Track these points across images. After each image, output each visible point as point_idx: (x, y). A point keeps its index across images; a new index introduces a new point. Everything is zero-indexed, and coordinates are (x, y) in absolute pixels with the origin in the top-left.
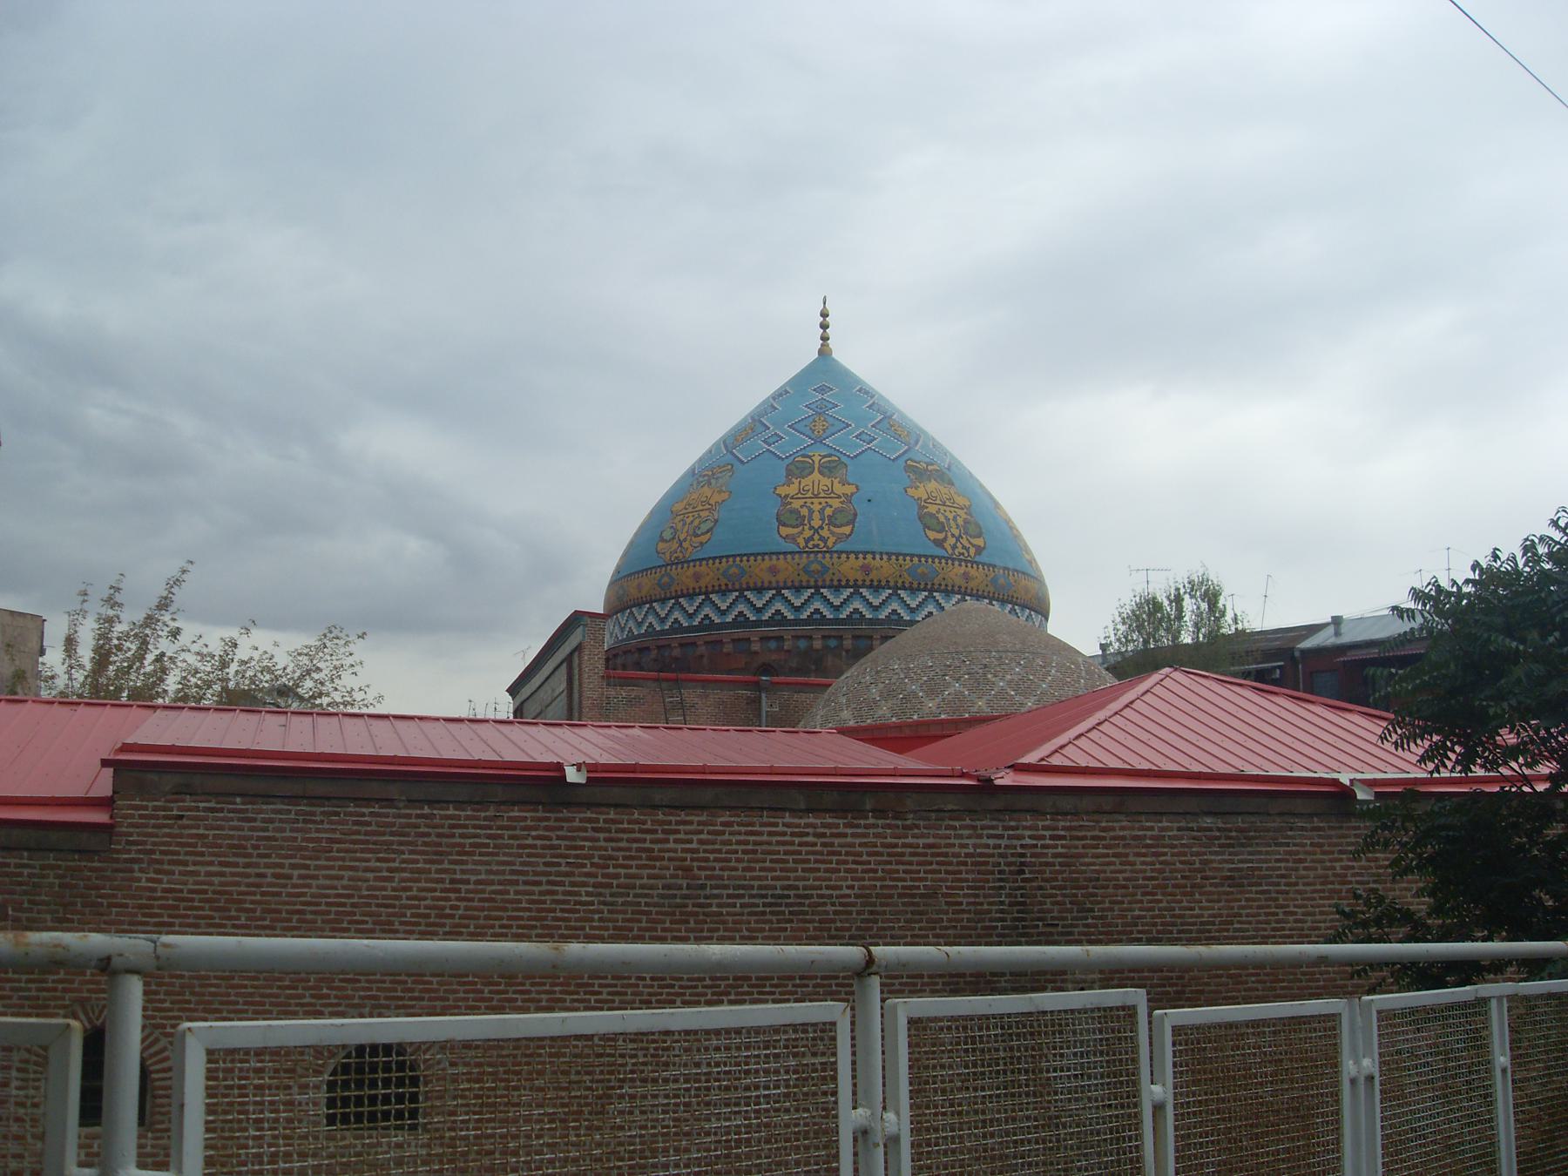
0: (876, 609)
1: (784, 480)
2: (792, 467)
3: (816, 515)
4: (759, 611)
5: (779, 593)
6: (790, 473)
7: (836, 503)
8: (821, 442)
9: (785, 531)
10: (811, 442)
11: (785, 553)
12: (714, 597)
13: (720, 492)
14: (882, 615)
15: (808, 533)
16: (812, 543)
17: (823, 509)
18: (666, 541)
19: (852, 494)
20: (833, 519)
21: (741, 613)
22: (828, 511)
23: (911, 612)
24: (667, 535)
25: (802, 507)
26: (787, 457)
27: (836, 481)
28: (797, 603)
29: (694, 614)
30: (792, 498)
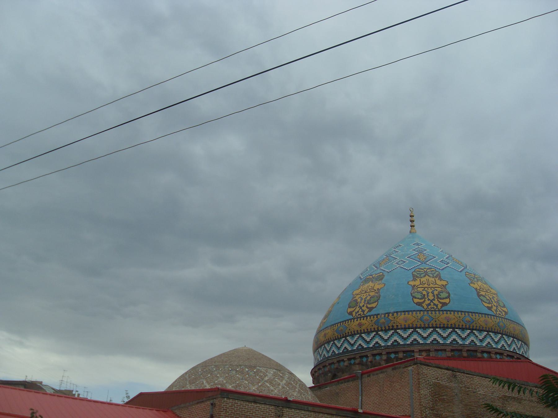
0: (386, 341)
3: (363, 301)
5: (346, 338)
7: (372, 294)
11: (348, 320)
14: (389, 343)
16: (358, 313)
17: (366, 298)
22: (368, 298)
23: (404, 340)
25: (359, 298)
30: (357, 295)
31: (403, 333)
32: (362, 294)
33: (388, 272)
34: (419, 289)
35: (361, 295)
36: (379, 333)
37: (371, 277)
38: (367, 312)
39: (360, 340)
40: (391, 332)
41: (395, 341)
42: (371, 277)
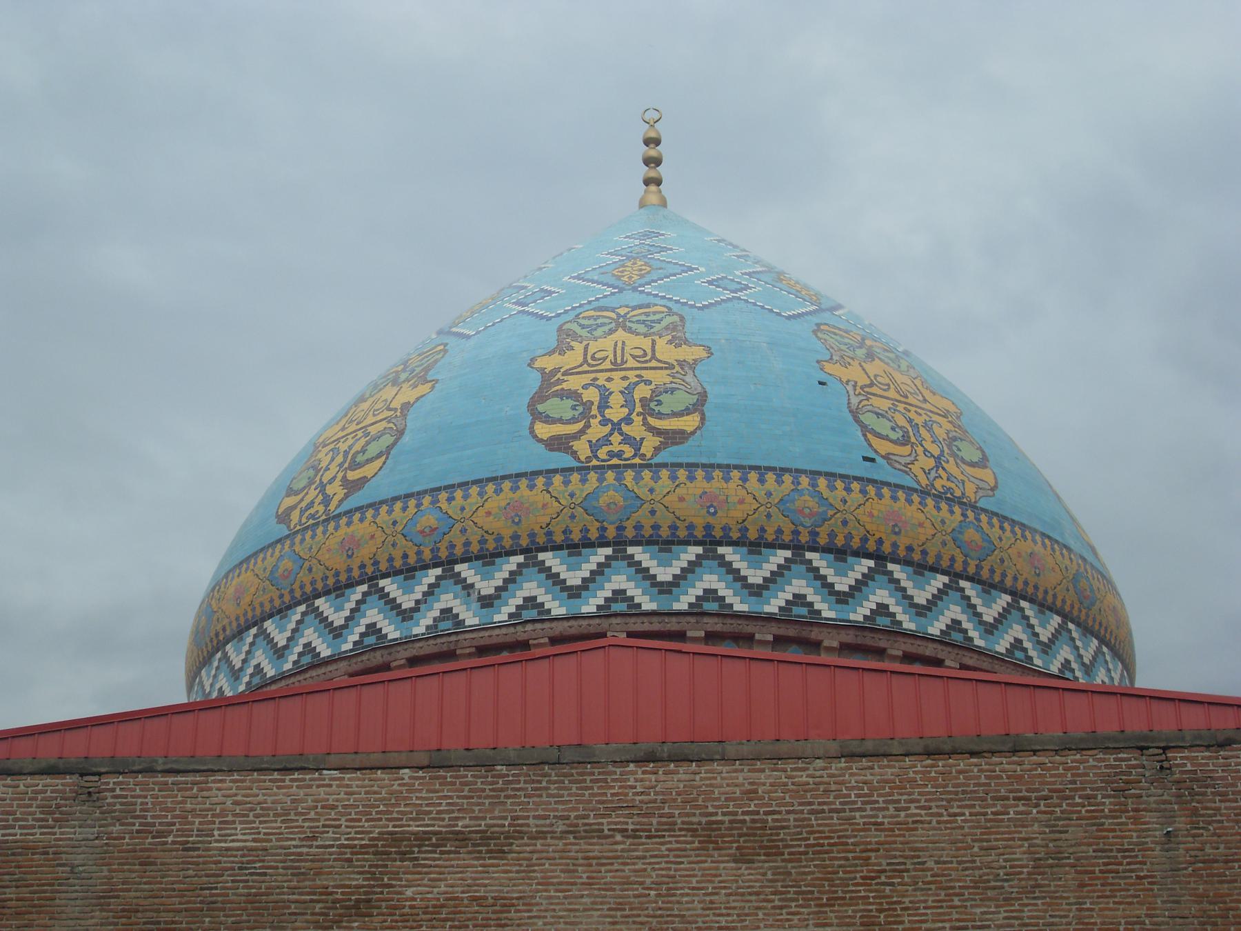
2: (575, 327)
3: (616, 400)
7: (660, 378)
8: (635, 289)
9: (543, 430)
12: (389, 586)
14: (772, 606)
15: (597, 431)
16: (605, 449)
20: (652, 405)
21: (447, 612)
22: (642, 392)
25: (585, 387)
26: (558, 315)
27: (661, 343)
28: (574, 579)
29: (345, 627)
30: (563, 375)
31: (831, 571)
32: (602, 371)
33: (699, 308)
34: (875, 401)
35: (593, 376)
37: (613, 315)
38: (657, 450)
40: (782, 555)
41: (799, 599)
42: (613, 315)
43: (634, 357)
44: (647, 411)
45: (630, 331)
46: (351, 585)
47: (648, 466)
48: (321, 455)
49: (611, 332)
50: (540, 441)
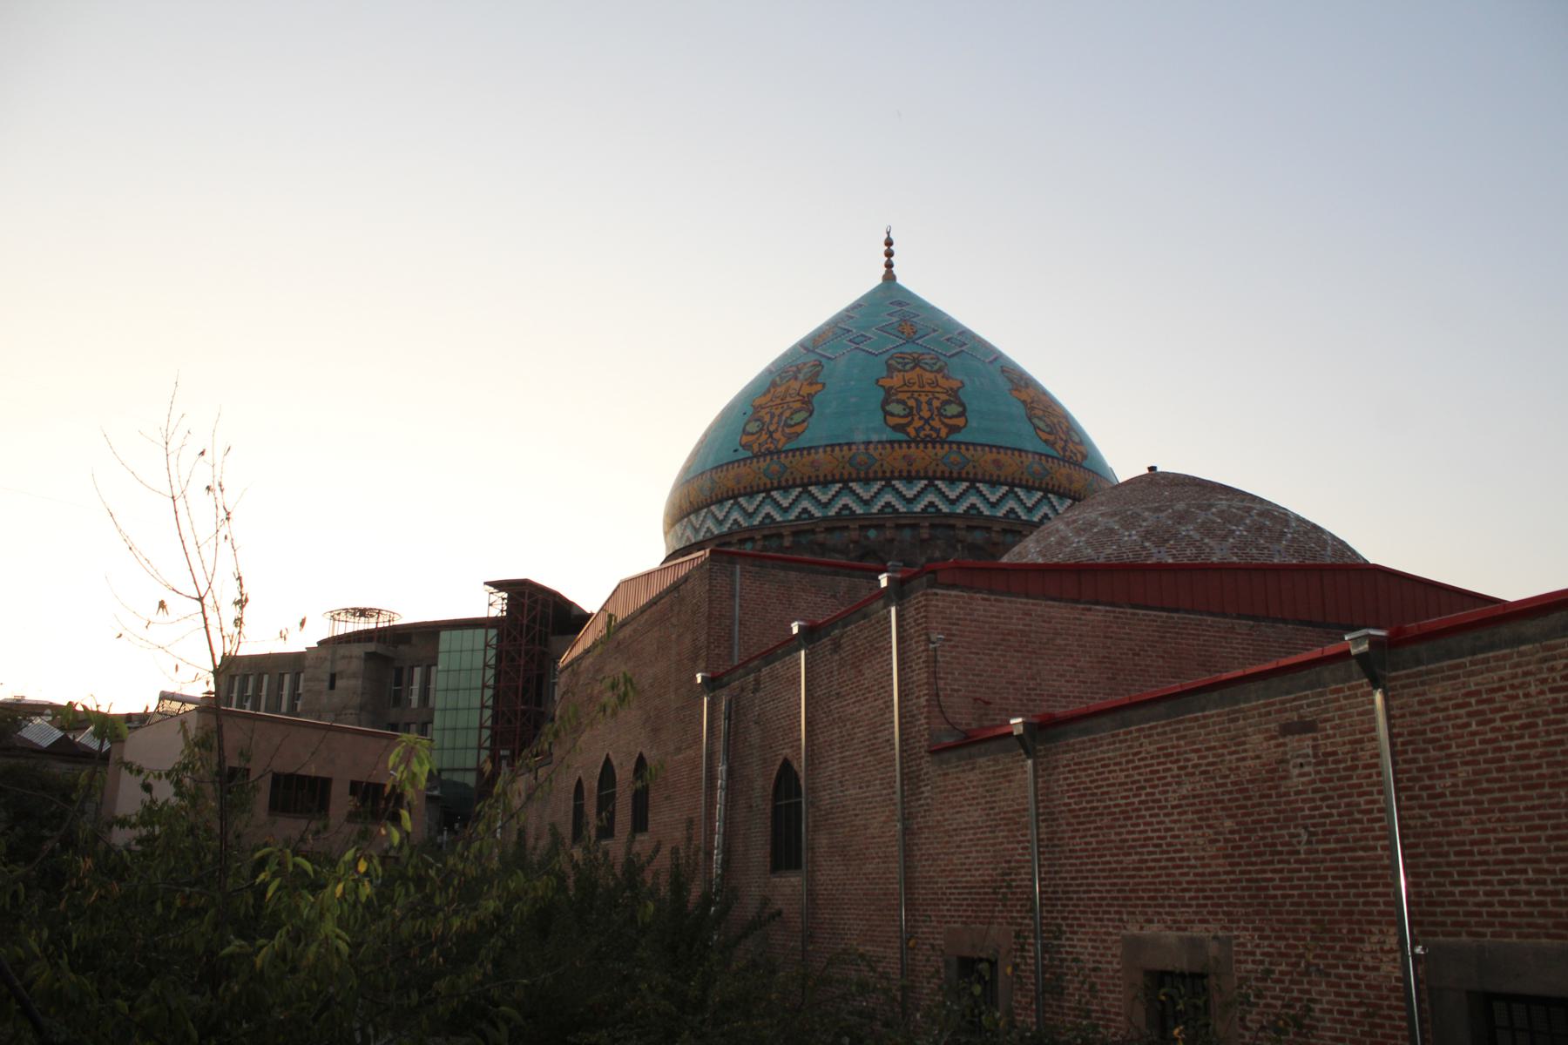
1: (885, 374)
2: (890, 362)
3: (925, 407)
4: (866, 503)
6: (890, 368)
8: (913, 342)
10: (901, 341)
11: (900, 442)
13: (811, 384)
15: (918, 423)
17: (929, 403)
18: (753, 434)
19: (959, 388)
22: (936, 403)
24: (753, 427)
25: (908, 398)
36: (937, 482)
38: (948, 435)
39: (931, 493)
43: (929, 384)
44: (940, 415)
45: (924, 369)
46: (795, 486)
47: (947, 442)
48: (760, 414)
49: (913, 368)
50: (890, 427)
